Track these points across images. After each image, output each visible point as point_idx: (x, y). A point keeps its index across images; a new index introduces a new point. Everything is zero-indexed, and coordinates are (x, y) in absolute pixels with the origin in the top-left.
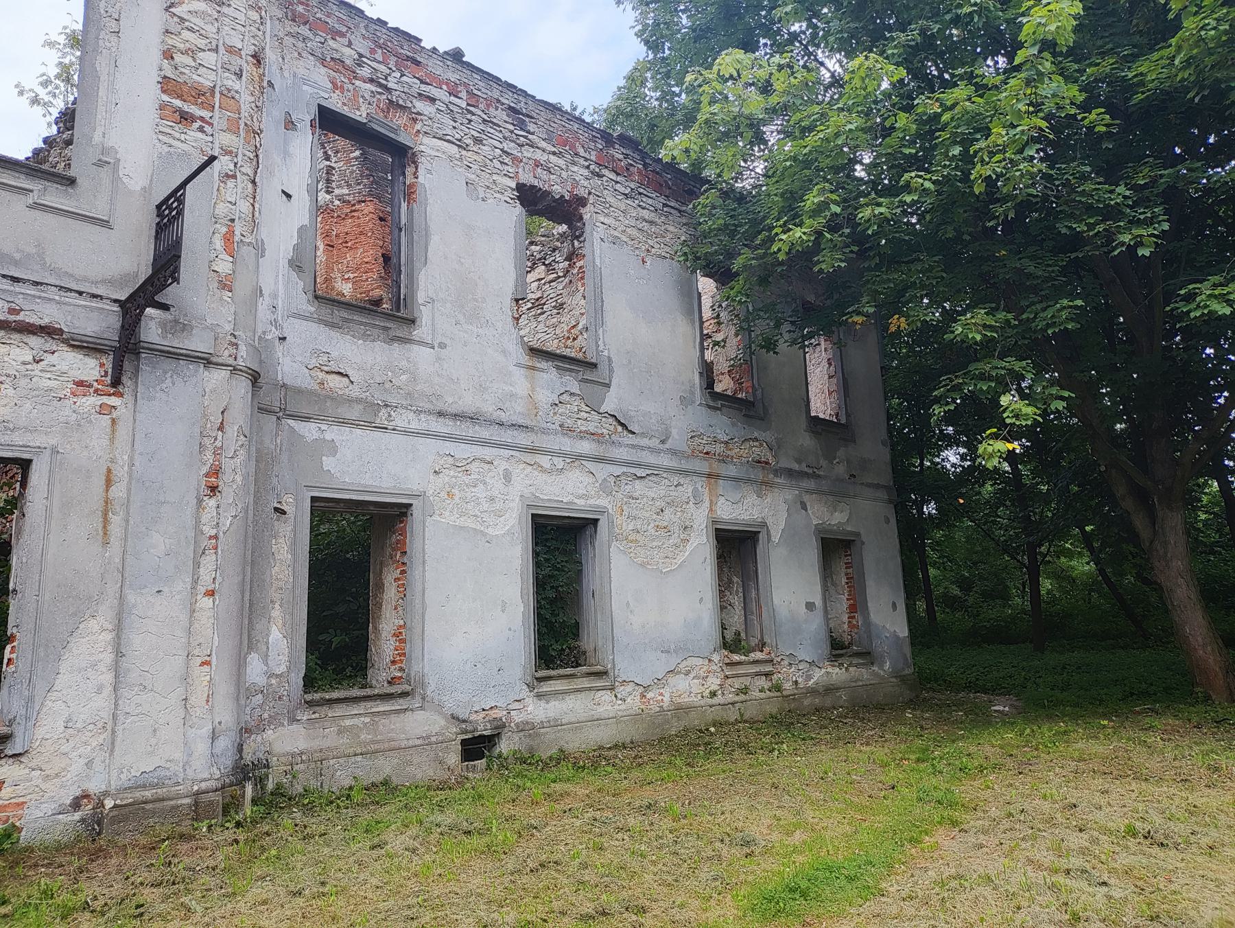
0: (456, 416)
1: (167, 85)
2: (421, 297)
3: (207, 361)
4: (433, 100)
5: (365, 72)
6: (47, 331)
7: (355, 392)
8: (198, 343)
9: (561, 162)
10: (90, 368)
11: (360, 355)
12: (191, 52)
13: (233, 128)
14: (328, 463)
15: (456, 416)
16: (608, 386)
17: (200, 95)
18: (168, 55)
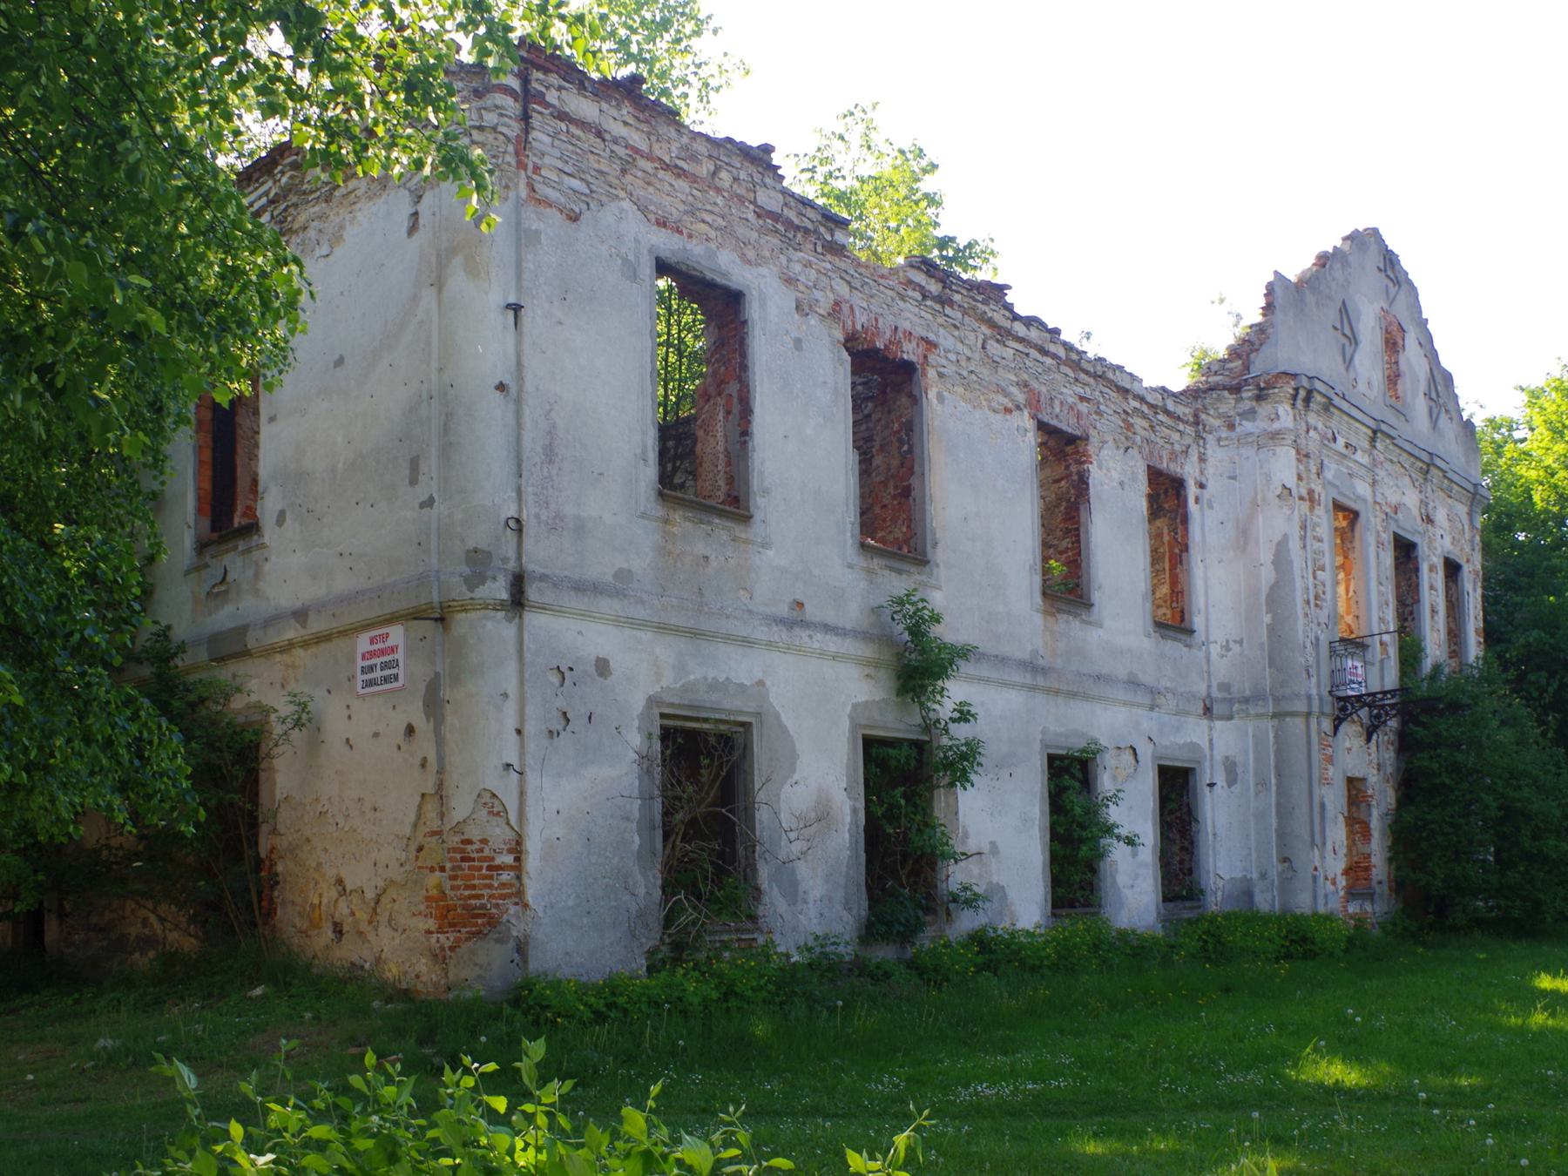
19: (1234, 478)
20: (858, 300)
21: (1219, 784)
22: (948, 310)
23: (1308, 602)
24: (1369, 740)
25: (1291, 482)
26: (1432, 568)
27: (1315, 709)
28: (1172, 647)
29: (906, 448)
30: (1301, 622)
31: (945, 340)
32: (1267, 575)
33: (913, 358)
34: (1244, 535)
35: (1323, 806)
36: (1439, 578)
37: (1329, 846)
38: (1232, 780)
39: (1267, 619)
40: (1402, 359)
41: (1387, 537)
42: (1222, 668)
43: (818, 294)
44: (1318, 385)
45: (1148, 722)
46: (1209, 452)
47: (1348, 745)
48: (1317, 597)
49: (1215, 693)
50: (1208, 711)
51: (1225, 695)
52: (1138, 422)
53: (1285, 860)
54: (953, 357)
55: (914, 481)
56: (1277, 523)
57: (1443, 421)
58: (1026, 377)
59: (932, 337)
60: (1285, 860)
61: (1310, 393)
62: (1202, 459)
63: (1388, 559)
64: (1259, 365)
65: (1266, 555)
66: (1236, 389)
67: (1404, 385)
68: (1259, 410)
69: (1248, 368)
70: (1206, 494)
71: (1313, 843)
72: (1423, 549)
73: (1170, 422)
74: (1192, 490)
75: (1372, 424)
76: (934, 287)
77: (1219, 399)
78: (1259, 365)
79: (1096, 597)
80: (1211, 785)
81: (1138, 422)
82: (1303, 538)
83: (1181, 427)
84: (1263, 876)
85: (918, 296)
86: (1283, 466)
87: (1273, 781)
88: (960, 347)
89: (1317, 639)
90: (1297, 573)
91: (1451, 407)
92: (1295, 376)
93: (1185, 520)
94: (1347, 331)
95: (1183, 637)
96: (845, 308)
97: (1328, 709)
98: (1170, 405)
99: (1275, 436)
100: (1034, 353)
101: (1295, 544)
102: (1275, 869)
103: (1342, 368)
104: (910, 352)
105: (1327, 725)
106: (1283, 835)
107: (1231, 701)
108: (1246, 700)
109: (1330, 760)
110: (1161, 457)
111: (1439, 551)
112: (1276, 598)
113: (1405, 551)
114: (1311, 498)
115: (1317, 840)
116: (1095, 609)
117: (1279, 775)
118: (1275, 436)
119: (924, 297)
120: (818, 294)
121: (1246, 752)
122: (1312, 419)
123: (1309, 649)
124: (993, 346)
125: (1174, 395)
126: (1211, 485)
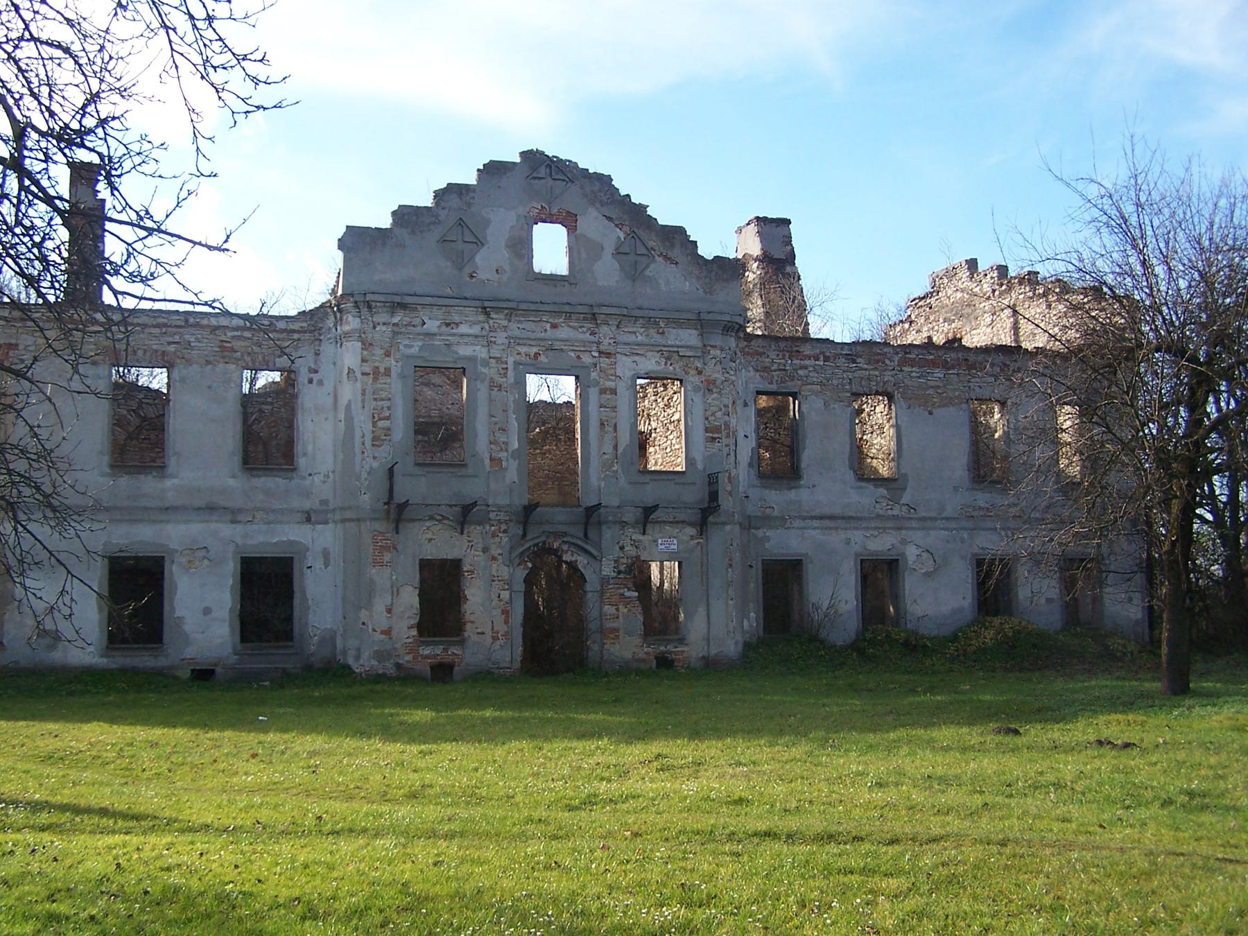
0: (821, 518)
1: (707, 430)
2: (803, 465)
3: (725, 524)
4: (806, 367)
5: (775, 367)
6: (683, 522)
7: (776, 513)
8: (723, 519)
9: (877, 373)
10: (691, 531)
11: (777, 498)
12: (713, 414)
13: (728, 436)
14: (767, 545)
15: (821, 518)
16: (904, 489)
17: (717, 429)
30: (358, 458)
45: (227, 530)
47: (430, 536)
48: (374, 439)
59: (13, 341)
62: (317, 354)
65: (342, 416)
70: (316, 377)
75: (478, 303)
82: (363, 401)
83: (296, 336)
109: (386, 548)
123: (364, 475)
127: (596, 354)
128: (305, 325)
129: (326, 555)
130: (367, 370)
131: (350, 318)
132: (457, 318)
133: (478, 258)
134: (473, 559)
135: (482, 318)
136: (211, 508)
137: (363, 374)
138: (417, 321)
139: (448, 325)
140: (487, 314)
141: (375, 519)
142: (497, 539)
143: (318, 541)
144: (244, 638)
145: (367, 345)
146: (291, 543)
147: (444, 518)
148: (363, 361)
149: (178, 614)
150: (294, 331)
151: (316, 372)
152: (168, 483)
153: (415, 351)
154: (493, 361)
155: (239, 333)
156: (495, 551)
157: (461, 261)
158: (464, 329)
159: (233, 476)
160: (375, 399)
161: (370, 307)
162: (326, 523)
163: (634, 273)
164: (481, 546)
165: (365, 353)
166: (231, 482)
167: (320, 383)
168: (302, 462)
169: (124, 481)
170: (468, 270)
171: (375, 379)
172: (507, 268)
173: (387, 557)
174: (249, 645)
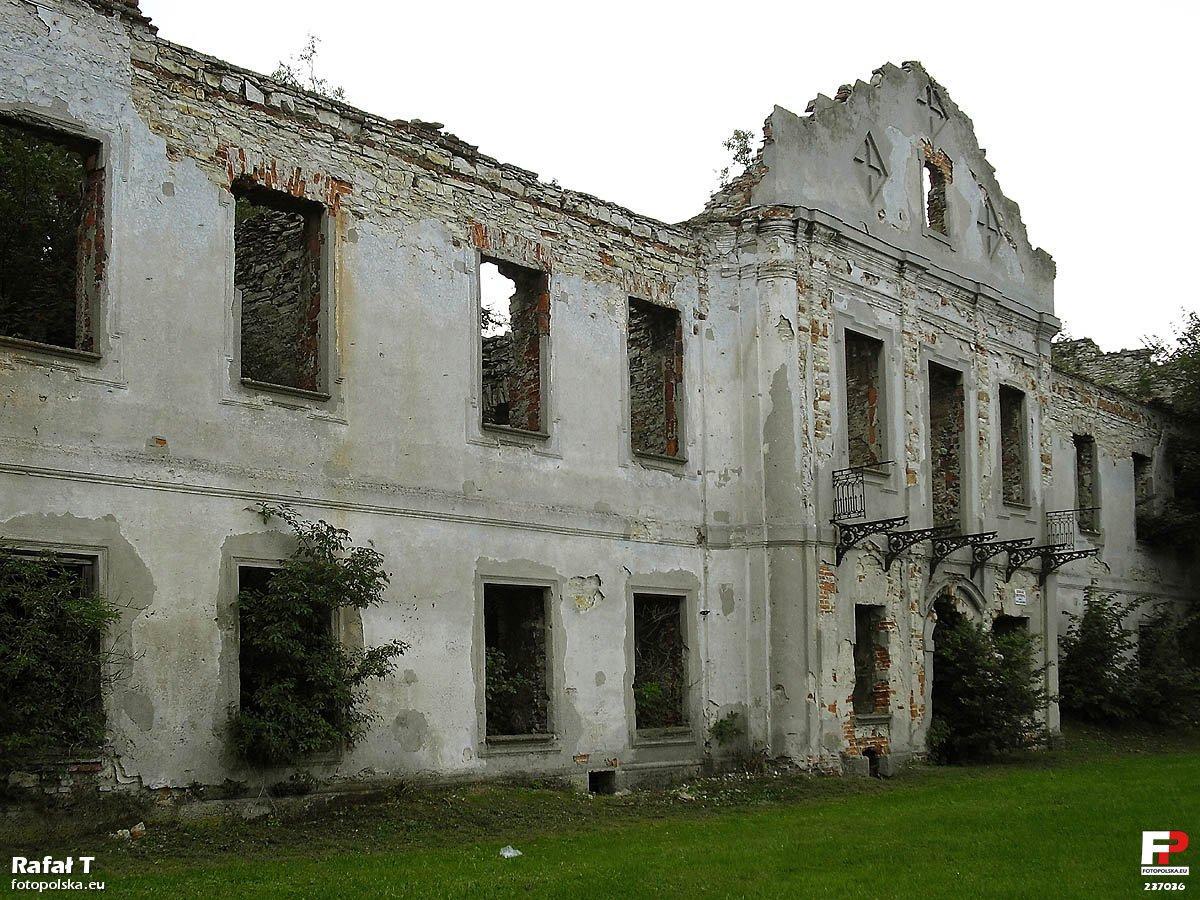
18: (1042, 445)
19: (735, 308)
20: (251, 146)
21: (714, 612)
22: (367, 150)
23: (806, 432)
24: (887, 568)
25: (791, 313)
26: (981, 396)
27: (812, 537)
28: (658, 477)
29: (314, 286)
30: (799, 452)
31: (362, 180)
32: (764, 404)
33: (320, 199)
34: (743, 367)
35: (819, 633)
36: (993, 409)
37: (827, 674)
38: (728, 606)
39: (764, 448)
40: (949, 189)
41: (920, 367)
42: (719, 497)
43: (197, 139)
44: (818, 217)
46: (710, 284)
49: (711, 522)
50: (702, 539)
51: (722, 524)
52: (618, 254)
53: (779, 687)
54: (373, 196)
55: (320, 316)
56: (782, 353)
57: (1005, 250)
58: (469, 213)
59: (346, 178)
60: (779, 687)
61: (811, 225)
63: (921, 388)
64: (761, 196)
65: (764, 387)
66: (736, 222)
67: (954, 216)
68: (759, 241)
69: (748, 200)
70: (705, 325)
71: (807, 671)
72: (970, 377)
73: (662, 253)
74: (688, 322)
76: (349, 128)
77: (720, 232)
78: (761, 196)
79: (554, 430)
80: (704, 613)
81: (618, 254)
82: (803, 369)
83: (677, 258)
84: (757, 703)
85: (329, 137)
86: (784, 298)
87: (768, 608)
88: (383, 186)
89: (816, 468)
90: (795, 402)
91: (1014, 235)
92: (794, 209)
93: (680, 350)
94: (874, 163)
95: (672, 467)
96: (232, 152)
97: (827, 538)
98: (663, 237)
99: (775, 268)
100: (480, 189)
101: (793, 376)
102: (768, 696)
103: (864, 200)
104: (314, 192)
105: (827, 554)
106: (775, 661)
107: (728, 531)
108: (742, 530)
109: (831, 588)
110: (649, 290)
111: (993, 378)
112: (775, 426)
113: (945, 383)
114: (815, 332)
115: (811, 665)
116: (554, 441)
117: (773, 603)
118: (775, 268)
119: (337, 138)
120: (197, 139)
121: (743, 580)
122: (817, 250)
123: (807, 480)
124: (427, 185)
125: (667, 227)
126: (709, 315)
127: (973, 347)
128: (685, 243)
129: (728, 598)
130: (805, 323)
131: (780, 243)
132: (875, 271)
133: (884, 193)
134: (894, 609)
135: (894, 276)
136: (603, 512)
137: (800, 329)
138: (843, 265)
139: (867, 276)
140: (901, 271)
141: (822, 543)
142: (912, 582)
143: (710, 578)
144: (638, 726)
145: (804, 287)
146: (683, 575)
147: (876, 549)
148: (801, 309)
149: (569, 683)
150: (673, 250)
151: (702, 317)
152: (549, 466)
153: (841, 306)
154: (906, 336)
155: (619, 238)
156: (914, 597)
157: (873, 194)
158: (882, 287)
159: (625, 466)
160: (816, 368)
161: (810, 231)
162: (727, 546)
163: (990, 250)
164: (899, 589)
165: (802, 298)
166: (622, 474)
167: (710, 334)
168: (692, 453)
169: (501, 455)
170: (878, 207)
171: (815, 339)
172: (907, 213)
173: (832, 599)
174: (647, 731)
